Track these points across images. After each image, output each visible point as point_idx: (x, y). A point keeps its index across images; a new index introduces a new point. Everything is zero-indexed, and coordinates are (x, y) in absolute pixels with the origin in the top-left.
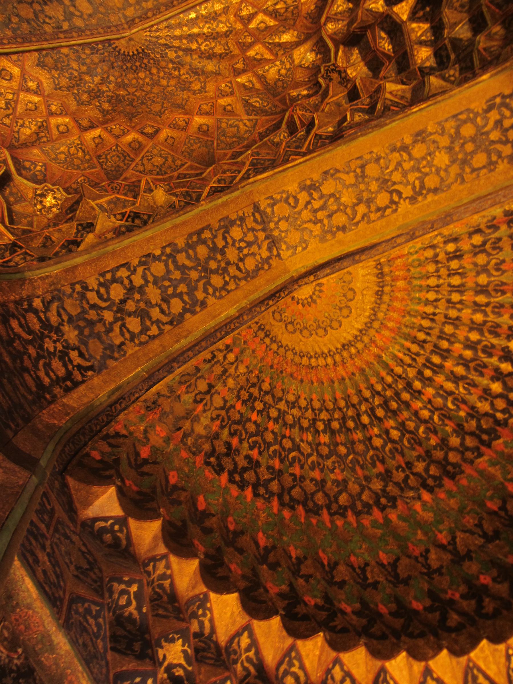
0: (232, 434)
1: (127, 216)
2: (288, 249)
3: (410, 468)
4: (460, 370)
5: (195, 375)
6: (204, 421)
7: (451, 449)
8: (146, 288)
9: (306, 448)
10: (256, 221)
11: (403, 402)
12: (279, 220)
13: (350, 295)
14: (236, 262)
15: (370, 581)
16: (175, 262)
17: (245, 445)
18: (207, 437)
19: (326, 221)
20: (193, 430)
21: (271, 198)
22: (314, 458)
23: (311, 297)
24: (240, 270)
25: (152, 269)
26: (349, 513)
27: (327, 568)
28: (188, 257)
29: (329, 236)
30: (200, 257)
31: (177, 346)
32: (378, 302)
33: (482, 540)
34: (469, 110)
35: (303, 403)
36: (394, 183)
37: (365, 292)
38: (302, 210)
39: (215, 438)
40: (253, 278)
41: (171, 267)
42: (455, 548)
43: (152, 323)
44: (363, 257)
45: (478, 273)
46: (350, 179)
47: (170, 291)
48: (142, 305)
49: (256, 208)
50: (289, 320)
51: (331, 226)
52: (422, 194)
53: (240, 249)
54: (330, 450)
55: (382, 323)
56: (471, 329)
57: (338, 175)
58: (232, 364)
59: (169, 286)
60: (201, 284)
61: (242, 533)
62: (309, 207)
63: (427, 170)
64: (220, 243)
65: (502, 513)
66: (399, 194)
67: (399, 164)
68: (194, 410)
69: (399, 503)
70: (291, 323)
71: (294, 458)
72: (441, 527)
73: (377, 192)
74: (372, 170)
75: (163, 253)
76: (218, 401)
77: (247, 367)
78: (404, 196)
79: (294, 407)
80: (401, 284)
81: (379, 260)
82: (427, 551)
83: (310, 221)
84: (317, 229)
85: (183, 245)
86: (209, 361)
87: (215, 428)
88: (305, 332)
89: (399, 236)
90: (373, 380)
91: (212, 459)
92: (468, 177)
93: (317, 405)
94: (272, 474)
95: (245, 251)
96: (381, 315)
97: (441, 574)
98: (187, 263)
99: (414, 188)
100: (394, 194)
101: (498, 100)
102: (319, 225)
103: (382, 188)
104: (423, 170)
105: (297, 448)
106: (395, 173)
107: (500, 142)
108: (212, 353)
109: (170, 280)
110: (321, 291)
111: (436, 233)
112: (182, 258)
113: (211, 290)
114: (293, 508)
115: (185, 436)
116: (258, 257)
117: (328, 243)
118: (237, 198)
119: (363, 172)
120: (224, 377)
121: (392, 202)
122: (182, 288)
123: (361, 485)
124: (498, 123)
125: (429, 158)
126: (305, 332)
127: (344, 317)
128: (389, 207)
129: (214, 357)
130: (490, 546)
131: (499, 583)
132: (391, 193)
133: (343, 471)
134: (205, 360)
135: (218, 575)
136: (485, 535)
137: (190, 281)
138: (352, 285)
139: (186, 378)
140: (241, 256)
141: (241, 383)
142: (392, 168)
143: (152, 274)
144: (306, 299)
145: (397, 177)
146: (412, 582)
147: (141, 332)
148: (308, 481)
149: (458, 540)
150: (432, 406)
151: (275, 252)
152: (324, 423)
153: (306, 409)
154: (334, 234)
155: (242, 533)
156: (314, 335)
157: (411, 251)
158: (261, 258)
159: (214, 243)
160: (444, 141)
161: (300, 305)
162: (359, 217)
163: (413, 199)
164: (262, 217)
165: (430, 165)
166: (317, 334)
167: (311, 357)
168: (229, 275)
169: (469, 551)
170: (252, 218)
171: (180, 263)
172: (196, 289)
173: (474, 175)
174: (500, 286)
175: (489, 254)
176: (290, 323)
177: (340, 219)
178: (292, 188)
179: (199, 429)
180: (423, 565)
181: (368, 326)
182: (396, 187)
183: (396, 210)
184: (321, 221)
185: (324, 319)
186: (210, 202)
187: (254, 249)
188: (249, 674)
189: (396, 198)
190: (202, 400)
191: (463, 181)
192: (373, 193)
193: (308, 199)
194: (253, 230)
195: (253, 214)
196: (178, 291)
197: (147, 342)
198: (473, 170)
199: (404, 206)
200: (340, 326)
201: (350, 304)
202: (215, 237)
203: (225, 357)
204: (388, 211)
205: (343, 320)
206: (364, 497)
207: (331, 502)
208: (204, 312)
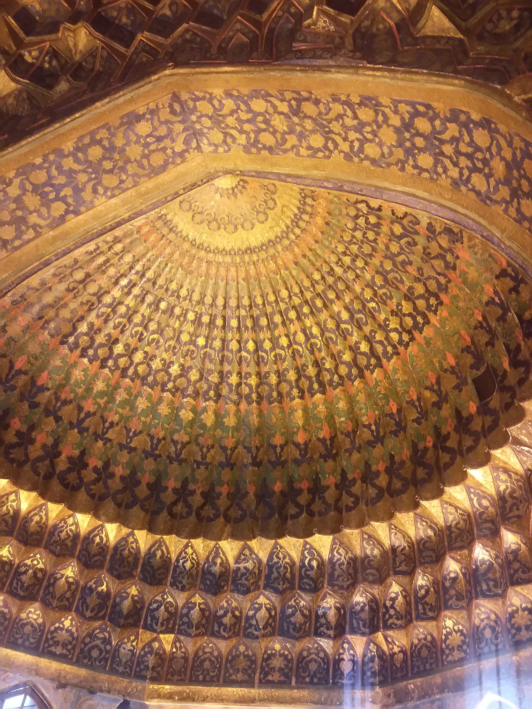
0: (98, 316)
1: (45, 52)
2: (210, 144)
3: (247, 379)
4: (331, 324)
5: (70, 267)
6: (73, 305)
7: (286, 381)
8: (24, 197)
9: (169, 332)
10: (173, 112)
11: (273, 323)
12: (202, 116)
13: (271, 204)
14: (138, 158)
15: (157, 452)
16: (59, 168)
17: (111, 324)
18: (70, 321)
19: (252, 135)
20: (57, 315)
21: (194, 94)
22: (172, 343)
23: (233, 189)
24: (143, 167)
25: (31, 179)
26: (179, 394)
27: (131, 434)
28: (77, 160)
29: (254, 150)
30: (90, 158)
31: (51, 249)
32: (294, 224)
33: (250, 460)
34: (428, 107)
35: (183, 292)
36: (331, 132)
37: (285, 209)
38: (227, 115)
39: (78, 321)
40: (157, 174)
41: (54, 172)
42: (231, 454)
43: (27, 230)
44: (289, 180)
45: (386, 257)
46: (283, 107)
47: (52, 196)
48: (19, 213)
49: (176, 97)
50: (200, 210)
51: (257, 141)
52: (359, 157)
53: (147, 145)
54: (191, 340)
55: (290, 245)
56: (357, 298)
57: (271, 99)
58: (117, 254)
59: (51, 191)
60: (89, 187)
61: (71, 402)
62: (235, 116)
63: (369, 136)
64: (119, 142)
65: (278, 450)
66: (336, 146)
67: (340, 117)
68: (62, 299)
69: (221, 401)
70: (201, 213)
71: (153, 340)
72: (235, 434)
73: (313, 132)
74: (308, 108)
75: (45, 161)
76: (92, 288)
77: (134, 256)
78: (340, 148)
79: (172, 295)
80: (319, 220)
81: (303, 190)
82: (213, 446)
83: (235, 128)
84: (242, 139)
85: (72, 149)
86: (91, 253)
87: (80, 313)
88: (214, 225)
89: (327, 180)
90: (257, 293)
91: (71, 339)
92: (409, 168)
93: (196, 297)
94: (126, 350)
95: (152, 147)
96: (293, 237)
97: (206, 468)
98: (76, 167)
99: (352, 147)
100: (330, 142)
101: (463, 117)
102: (244, 136)
103: (318, 131)
104: (365, 134)
105: (160, 331)
106: (335, 123)
107: (450, 158)
108: (96, 244)
109: (52, 185)
110: (244, 187)
111: (364, 198)
112: (69, 163)
113: (101, 190)
114: (132, 380)
115: (47, 322)
116: (169, 151)
117: (252, 156)
118: (149, 91)
119: (299, 106)
120: (104, 268)
121: (326, 147)
122: (67, 191)
123: (201, 375)
124: (455, 140)
125: (375, 127)
126: (214, 225)
127: (258, 221)
128: (322, 151)
129: (98, 248)
130: (250, 468)
131: (228, 498)
132: (327, 139)
133: (192, 359)
134: (87, 252)
135: (11, 456)
136: (254, 458)
137: (78, 184)
138: (274, 196)
139: (60, 270)
140: (146, 151)
141: (122, 272)
142: (331, 115)
143: (31, 183)
144: (227, 189)
145: (336, 127)
146: (183, 464)
147: (17, 237)
148: (158, 360)
149: (237, 451)
150: (294, 338)
151: (194, 144)
152: (196, 316)
153: (185, 299)
154: (259, 150)
155: (71, 402)
156: (222, 230)
157: (336, 199)
158: (174, 152)
159: (111, 143)
160: (396, 121)
161: (218, 194)
162: (288, 146)
163: (348, 157)
164: (182, 107)
165: (375, 134)
166: (225, 229)
167: (210, 251)
168: (126, 172)
169: (235, 464)
170: (168, 110)
171: (65, 168)
172: (83, 190)
173: (416, 172)
174: (398, 282)
175: (401, 248)
176: (199, 213)
177: (267, 139)
178: (218, 92)
179: (65, 314)
180: (202, 456)
181: (279, 239)
182: (333, 136)
183: (329, 157)
184: (247, 133)
185: (239, 216)
186: (108, 103)
187: (167, 142)
188: (9, 513)
189: (330, 145)
190: (74, 289)
191: (403, 169)
192: (307, 130)
193: (235, 107)
194: (167, 122)
195: (171, 106)
196: (62, 194)
197: (21, 246)
198: (416, 167)
199: (337, 157)
200: (252, 228)
201: (268, 211)
202: (113, 135)
203: (110, 248)
204: (320, 154)
205: (257, 223)
206: (198, 385)
207: (169, 380)
208: (91, 212)
